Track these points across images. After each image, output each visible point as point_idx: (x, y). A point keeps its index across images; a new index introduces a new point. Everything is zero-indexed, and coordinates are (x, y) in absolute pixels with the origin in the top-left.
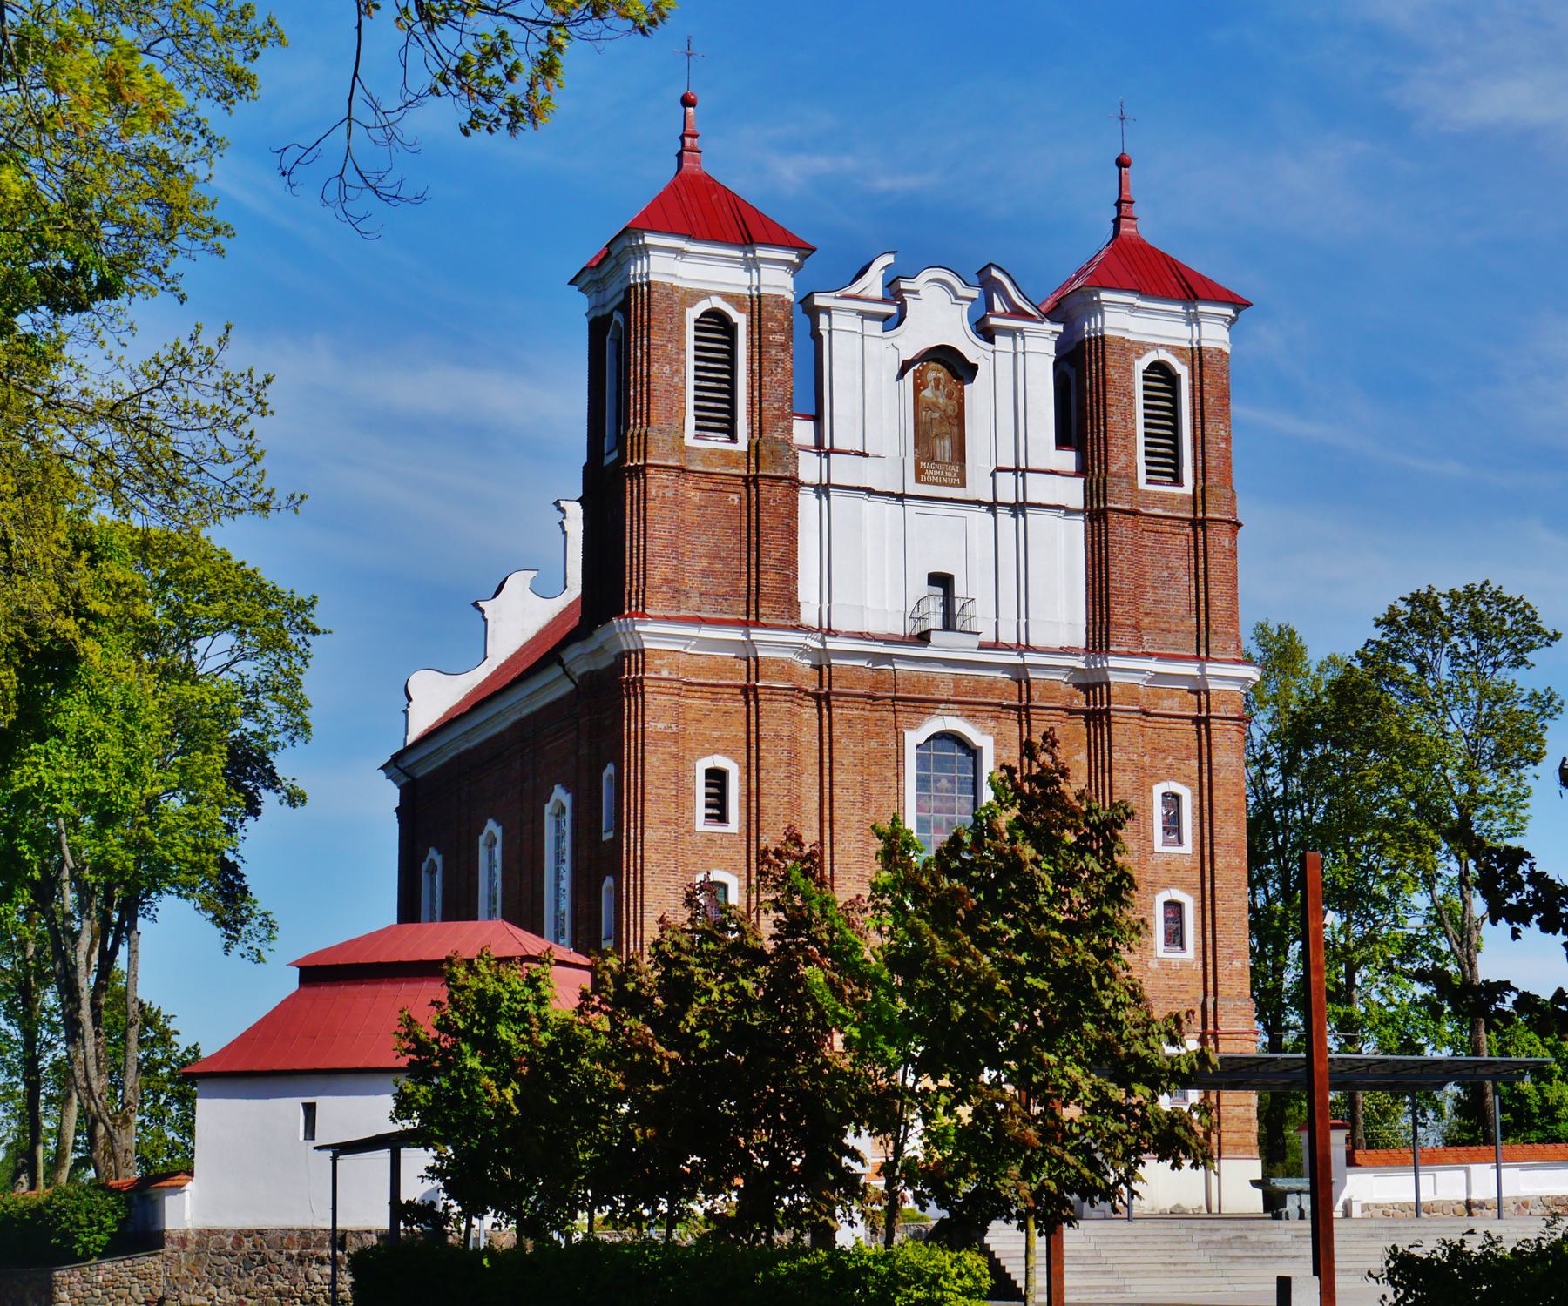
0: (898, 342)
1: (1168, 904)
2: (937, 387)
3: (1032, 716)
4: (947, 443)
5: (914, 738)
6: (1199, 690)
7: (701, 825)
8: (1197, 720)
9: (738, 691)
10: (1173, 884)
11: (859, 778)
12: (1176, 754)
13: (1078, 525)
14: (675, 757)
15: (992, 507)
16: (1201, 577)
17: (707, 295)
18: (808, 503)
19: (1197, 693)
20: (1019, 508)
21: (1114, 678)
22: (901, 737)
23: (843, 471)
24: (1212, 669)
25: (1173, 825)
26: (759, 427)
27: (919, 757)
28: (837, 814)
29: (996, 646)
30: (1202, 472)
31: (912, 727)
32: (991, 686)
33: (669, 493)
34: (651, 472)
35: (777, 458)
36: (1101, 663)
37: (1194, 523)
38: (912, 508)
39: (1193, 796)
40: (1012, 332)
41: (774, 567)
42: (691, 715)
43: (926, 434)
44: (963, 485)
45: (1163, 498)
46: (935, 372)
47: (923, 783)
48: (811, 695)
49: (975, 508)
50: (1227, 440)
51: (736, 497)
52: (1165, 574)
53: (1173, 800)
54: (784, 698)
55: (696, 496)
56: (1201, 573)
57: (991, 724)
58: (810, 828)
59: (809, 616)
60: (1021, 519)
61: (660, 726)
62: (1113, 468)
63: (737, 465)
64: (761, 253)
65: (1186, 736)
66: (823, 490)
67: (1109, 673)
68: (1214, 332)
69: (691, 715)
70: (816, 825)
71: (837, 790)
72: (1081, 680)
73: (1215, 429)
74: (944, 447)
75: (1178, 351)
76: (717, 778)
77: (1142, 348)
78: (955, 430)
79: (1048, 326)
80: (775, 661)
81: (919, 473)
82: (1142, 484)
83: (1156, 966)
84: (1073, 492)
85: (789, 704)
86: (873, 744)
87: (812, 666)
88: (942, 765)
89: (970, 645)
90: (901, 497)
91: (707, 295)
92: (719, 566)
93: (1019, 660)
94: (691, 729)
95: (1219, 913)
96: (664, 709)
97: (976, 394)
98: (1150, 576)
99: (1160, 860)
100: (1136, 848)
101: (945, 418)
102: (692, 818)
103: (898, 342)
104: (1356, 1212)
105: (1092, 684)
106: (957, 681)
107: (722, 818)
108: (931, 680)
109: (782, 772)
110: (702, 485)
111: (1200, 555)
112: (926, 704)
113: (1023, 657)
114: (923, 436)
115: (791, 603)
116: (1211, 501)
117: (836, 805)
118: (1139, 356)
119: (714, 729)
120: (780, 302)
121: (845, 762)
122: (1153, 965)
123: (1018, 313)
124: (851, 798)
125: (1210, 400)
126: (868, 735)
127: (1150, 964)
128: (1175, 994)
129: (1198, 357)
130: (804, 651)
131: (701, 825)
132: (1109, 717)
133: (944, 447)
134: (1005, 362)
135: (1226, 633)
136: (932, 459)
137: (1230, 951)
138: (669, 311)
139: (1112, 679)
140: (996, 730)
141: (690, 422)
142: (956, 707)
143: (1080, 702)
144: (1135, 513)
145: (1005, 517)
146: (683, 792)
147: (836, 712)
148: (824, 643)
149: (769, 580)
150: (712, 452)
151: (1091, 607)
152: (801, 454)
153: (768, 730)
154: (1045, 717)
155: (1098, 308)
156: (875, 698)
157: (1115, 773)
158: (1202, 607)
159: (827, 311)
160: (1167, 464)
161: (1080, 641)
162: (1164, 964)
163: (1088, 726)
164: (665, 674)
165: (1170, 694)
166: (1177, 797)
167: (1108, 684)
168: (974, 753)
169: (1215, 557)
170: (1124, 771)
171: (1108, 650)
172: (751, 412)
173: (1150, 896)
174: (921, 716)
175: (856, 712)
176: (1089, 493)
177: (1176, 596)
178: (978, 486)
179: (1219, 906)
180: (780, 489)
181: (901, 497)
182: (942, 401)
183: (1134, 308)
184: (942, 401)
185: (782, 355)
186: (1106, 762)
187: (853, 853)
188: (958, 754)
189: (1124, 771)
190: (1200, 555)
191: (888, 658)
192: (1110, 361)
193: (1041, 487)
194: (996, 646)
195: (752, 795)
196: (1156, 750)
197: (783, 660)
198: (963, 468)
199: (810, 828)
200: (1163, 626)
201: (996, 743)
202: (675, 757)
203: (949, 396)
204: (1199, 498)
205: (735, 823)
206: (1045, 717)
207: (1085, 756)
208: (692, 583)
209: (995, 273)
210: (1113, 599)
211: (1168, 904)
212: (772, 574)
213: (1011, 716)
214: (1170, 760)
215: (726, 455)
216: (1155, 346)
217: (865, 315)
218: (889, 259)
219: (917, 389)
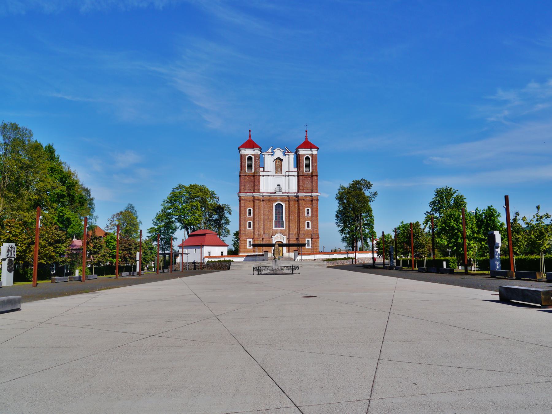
0: (274, 157)
1: (307, 223)
2: (278, 162)
4: (280, 169)
5: (274, 204)
6: (311, 196)
7: (248, 216)
8: (311, 200)
10: (308, 220)
13: (296, 177)
14: (244, 208)
15: (285, 176)
16: (312, 183)
17: (249, 154)
18: (261, 177)
19: (311, 197)
20: (288, 176)
21: (300, 196)
23: (266, 173)
24: (312, 194)
25: (308, 213)
26: (255, 169)
27: (275, 207)
29: (286, 193)
30: (313, 170)
31: (274, 203)
32: (285, 198)
33: (244, 178)
34: (242, 176)
35: (257, 173)
37: (312, 176)
40: (288, 155)
42: (247, 203)
43: (277, 168)
44: (282, 174)
45: (307, 173)
46: (278, 160)
47: (276, 209)
48: (262, 200)
50: (317, 165)
53: (308, 210)
55: (247, 178)
59: (261, 191)
61: (243, 205)
62: (300, 170)
63: (252, 174)
64: (255, 149)
65: (310, 202)
66: (263, 176)
68: (315, 152)
69: (247, 203)
70: (263, 215)
72: (296, 196)
73: (315, 164)
74: (279, 169)
75: (310, 155)
76: (250, 210)
77: (304, 155)
79: (292, 154)
80: (256, 197)
81: (276, 173)
82: (305, 172)
84: (296, 174)
86: (270, 205)
88: (279, 207)
90: (273, 176)
91: (249, 154)
92: (250, 186)
93: (287, 194)
94: (247, 205)
95: (314, 223)
98: (306, 183)
99: (306, 217)
101: (280, 166)
102: (247, 215)
103: (274, 157)
104: (298, 260)
105: (297, 197)
106: (280, 197)
107: (251, 215)
108: (277, 197)
109: (257, 209)
111: (312, 180)
112: (276, 200)
114: (277, 168)
115: (259, 189)
116: (313, 173)
118: (305, 156)
120: (258, 154)
122: (305, 230)
123: (289, 152)
125: (314, 161)
126: (269, 204)
129: (312, 155)
130: (260, 195)
131: (248, 216)
133: (279, 169)
134: (287, 158)
136: (278, 171)
138: (244, 157)
141: (247, 169)
143: (296, 199)
144: (303, 176)
145: (287, 177)
146: (246, 212)
147: (265, 202)
149: (256, 187)
150: (249, 173)
152: (261, 172)
155: (299, 151)
156: (270, 200)
158: (312, 186)
159: (264, 155)
160: (308, 168)
161: (296, 192)
162: (306, 230)
164: (243, 199)
165: (308, 197)
166: (309, 210)
168: (283, 205)
169: (314, 180)
172: (254, 168)
176: (298, 174)
177: (309, 185)
178: (284, 174)
179: (314, 223)
180: (257, 177)
181: (273, 176)
182: (279, 164)
183: (303, 150)
184: (279, 164)
190: (312, 180)
191: (271, 195)
192: (300, 157)
193: (291, 174)
194: (286, 193)
195: (254, 212)
196: (306, 204)
198: (282, 172)
201: (285, 204)
202: (244, 208)
203: (280, 163)
204: (312, 173)
205: (252, 215)
208: (247, 188)
209: (286, 148)
210: (300, 186)
211: (307, 223)
215: (251, 173)
216: (307, 155)
217: (269, 155)
218: (272, 148)
219: (276, 163)
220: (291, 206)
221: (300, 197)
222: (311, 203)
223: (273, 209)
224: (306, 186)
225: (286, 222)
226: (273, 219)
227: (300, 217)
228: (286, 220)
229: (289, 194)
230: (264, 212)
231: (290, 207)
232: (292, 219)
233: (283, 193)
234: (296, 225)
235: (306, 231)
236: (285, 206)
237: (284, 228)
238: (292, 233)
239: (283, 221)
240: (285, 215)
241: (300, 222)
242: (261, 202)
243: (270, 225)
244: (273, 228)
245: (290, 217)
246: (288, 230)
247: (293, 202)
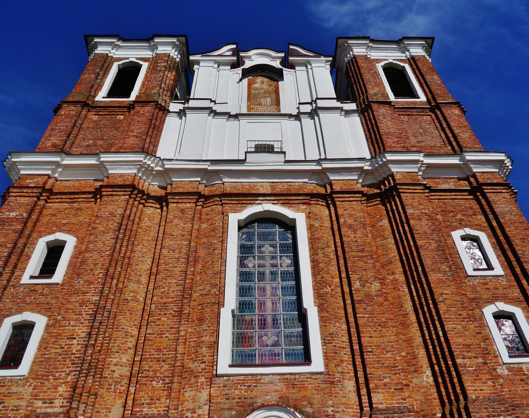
3: (336, 199)
9: (91, 196)
11: (186, 243)
12: (463, 213)
21: (394, 169)
22: (226, 218)
28: (162, 267)
31: (236, 211)
36: (382, 160)
38: (244, 121)
39: (489, 237)
49: (287, 118)
51: (122, 117)
54: (122, 193)
56: (445, 125)
57: (303, 207)
58: (139, 282)
60: (316, 118)
67: (390, 166)
71: (164, 252)
83: (506, 372)
86: (204, 226)
87: (160, 187)
89: (278, 160)
100: (447, 269)
109: (111, 235)
113: (321, 166)
117: (162, 261)
121: (174, 233)
124: (177, 256)
127: (499, 371)
132: (397, 190)
139: (393, 170)
140: (308, 210)
142: (272, 198)
147: (171, 206)
148: (163, 165)
151: (371, 147)
153: (105, 212)
154: (346, 199)
157: (412, 222)
163: (384, 205)
167: (392, 175)
170: (420, 220)
171: (384, 150)
173: (477, 311)
174: (245, 205)
175: (188, 205)
186: (403, 217)
187: (172, 295)
188: (277, 229)
197: (128, 175)
199: (139, 282)
201: (308, 217)
206: (346, 199)
207: (387, 222)
213: (320, 203)
214: (459, 216)
220: (350, 221)
221: (397, 177)
222: (477, 207)
223: (223, 241)
225: (323, 321)
226: (220, 304)
227: (433, 277)
228: (321, 308)
229: (326, 165)
230: (156, 261)
231: (344, 230)
232: (368, 296)
233: (286, 162)
234: (409, 341)
236: (310, 228)
238: (395, 403)
240: (314, 275)
241: (442, 307)
242: (149, 211)
243: (199, 345)
244: (214, 363)
245: (357, 285)
246: (350, 385)
247: (357, 206)
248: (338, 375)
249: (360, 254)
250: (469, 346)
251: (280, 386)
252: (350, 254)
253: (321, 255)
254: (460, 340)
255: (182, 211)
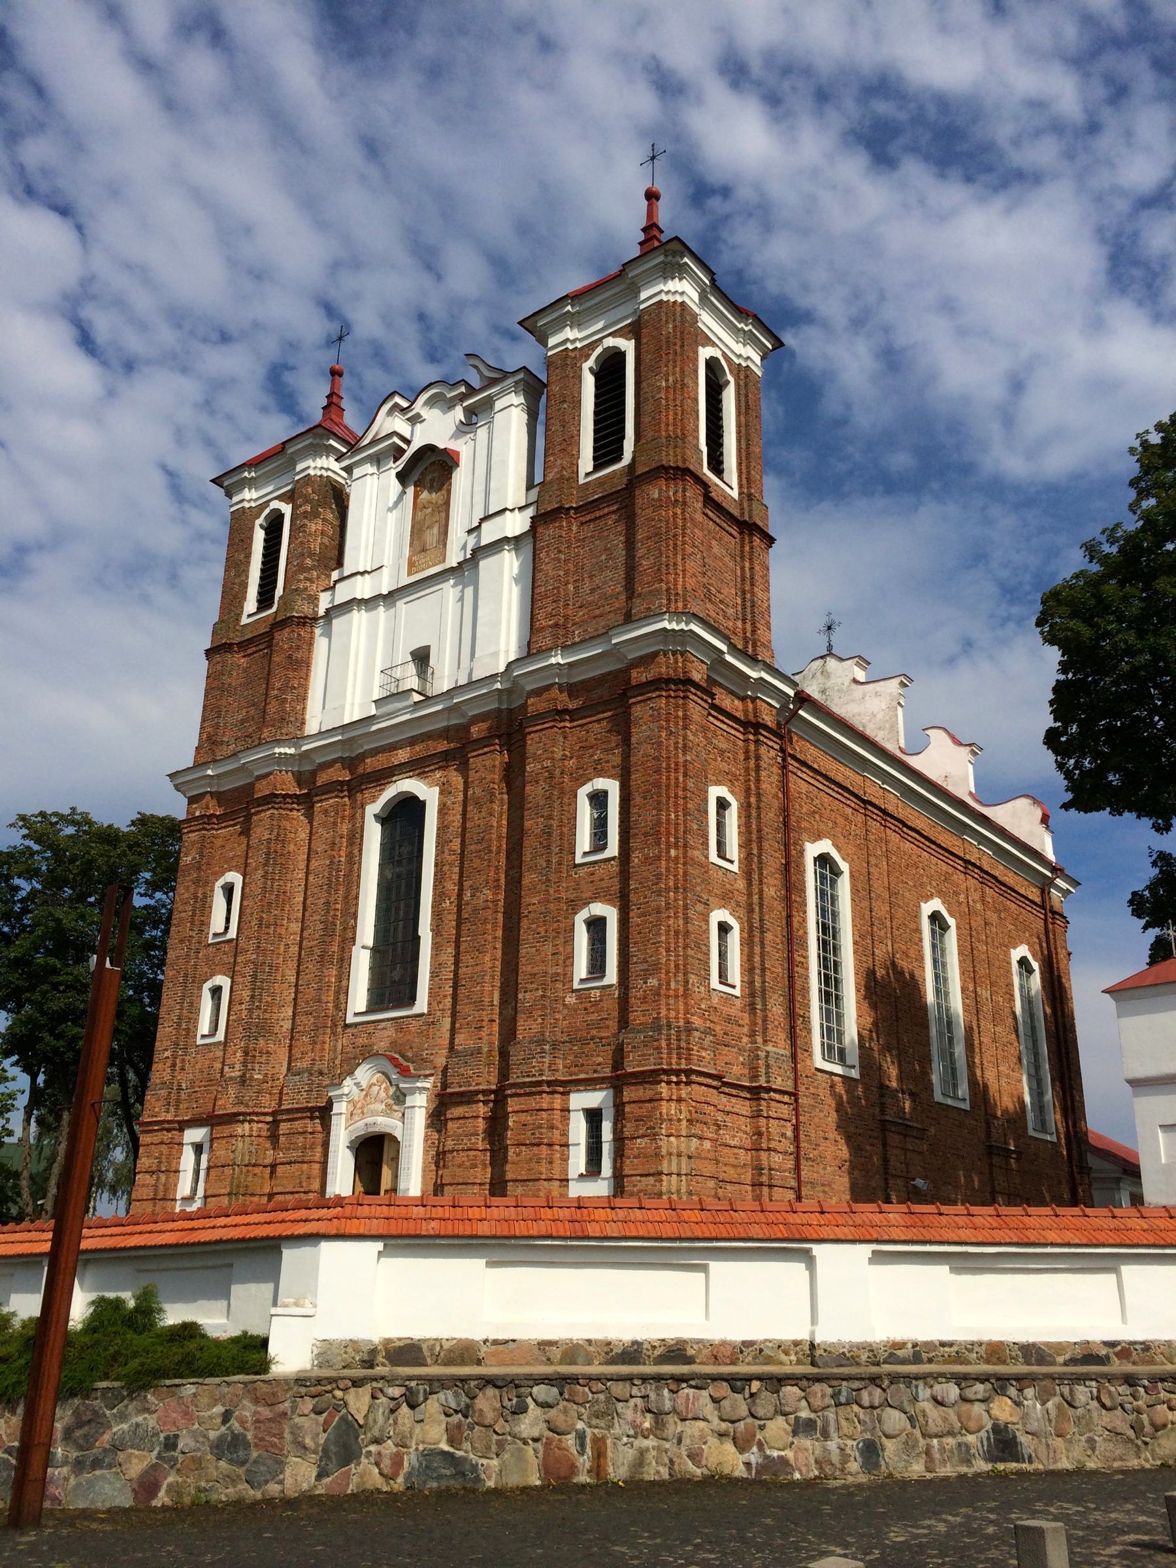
4: (435, 530)
5: (373, 809)
10: (595, 898)
31: (374, 799)
41: (276, 697)
52: (604, 557)
74: (432, 536)
78: (443, 515)
85: (272, 811)
96: (193, 843)
97: (461, 479)
110: (249, 651)
112: (384, 776)
118: (588, 357)
119: (231, 850)
128: (594, 1032)
135: (650, 592)
137: (645, 966)
185: (306, 521)
189: (537, 782)
198: (445, 545)
200: (597, 612)
212: (274, 702)
224: (592, 591)
225: (437, 947)
228: (437, 930)
232: (476, 910)
235: (573, 1010)
236: (443, 810)
237: (422, 1004)
239: (417, 939)
241: (524, 923)
248: (439, 1013)
249: (479, 847)
250: (535, 975)
251: (391, 1032)
252: (473, 847)
253: (447, 852)
254: (529, 969)
255: (326, 812)
